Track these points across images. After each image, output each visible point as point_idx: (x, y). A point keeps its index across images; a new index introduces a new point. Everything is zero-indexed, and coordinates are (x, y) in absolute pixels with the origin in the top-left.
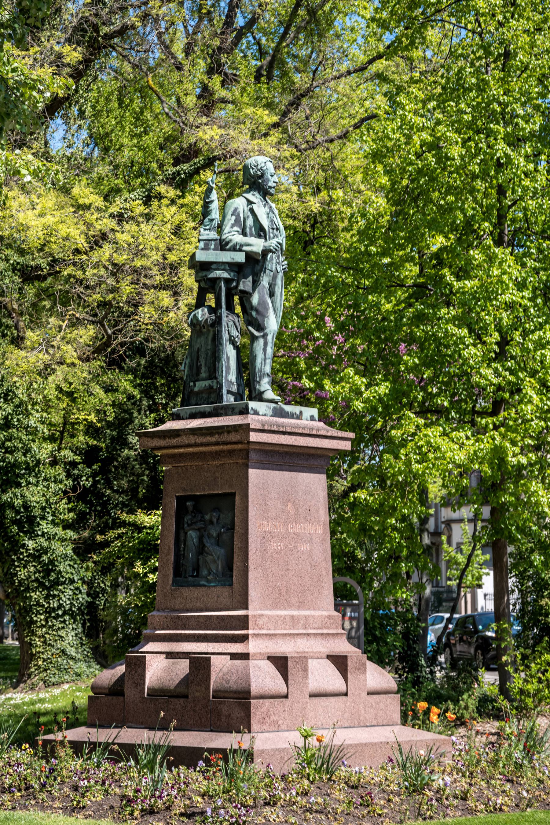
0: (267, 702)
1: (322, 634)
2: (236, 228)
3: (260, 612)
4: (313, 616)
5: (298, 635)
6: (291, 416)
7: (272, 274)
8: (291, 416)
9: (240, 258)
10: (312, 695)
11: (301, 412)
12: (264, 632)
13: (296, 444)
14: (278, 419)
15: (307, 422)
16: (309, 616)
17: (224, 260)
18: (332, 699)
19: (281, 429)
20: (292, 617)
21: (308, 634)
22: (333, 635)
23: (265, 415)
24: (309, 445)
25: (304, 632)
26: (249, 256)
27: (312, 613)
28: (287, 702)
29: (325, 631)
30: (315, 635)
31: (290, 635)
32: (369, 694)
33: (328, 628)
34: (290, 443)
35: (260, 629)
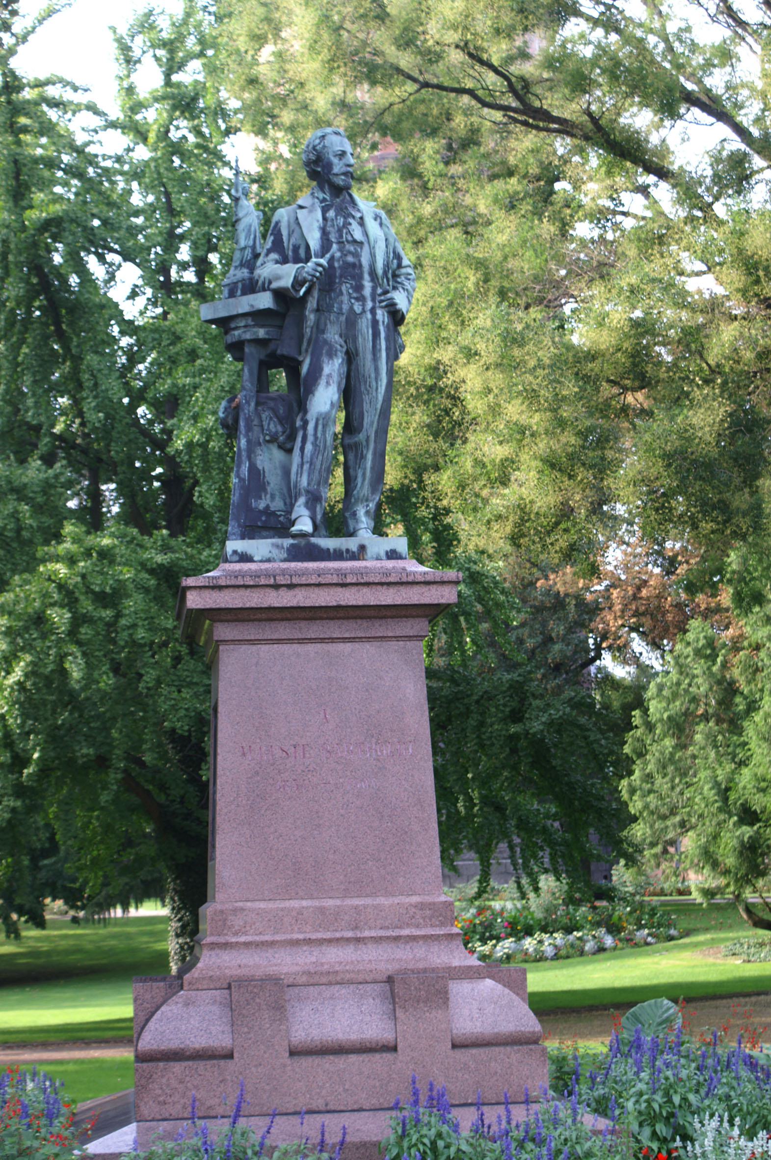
0: (177, 1067)
1: (397, 939)
2: (274, 256)
3: (240, 904)
4: (375, 907)
5: (330, 941)
6: (338, 555)
7: (343, 318)
8: (338, 555)
9: (264, 301)
10: (293, 1053)
11: (362, 548)
12: (242, 939)
13: (308, 603)
14: (293, 565)
15: (378, 564)
16: (365, 907)
17: (241, 311)
18: (353, 1058)
19: (263, 582)
20: (322, 910)
21: (358, 940)
22: (425, 938)
23: (269, 560)
24: (343, 603)
25: (350, 934)
26: (280, 295)
27: (368, 901)
28: (230, 1064)
29: (406, 932)
30: (378, 940)
31: (309, 942)
32: (454, 1046)
33: (417, 926)
34: (294, 603)
35: (236, 934)
